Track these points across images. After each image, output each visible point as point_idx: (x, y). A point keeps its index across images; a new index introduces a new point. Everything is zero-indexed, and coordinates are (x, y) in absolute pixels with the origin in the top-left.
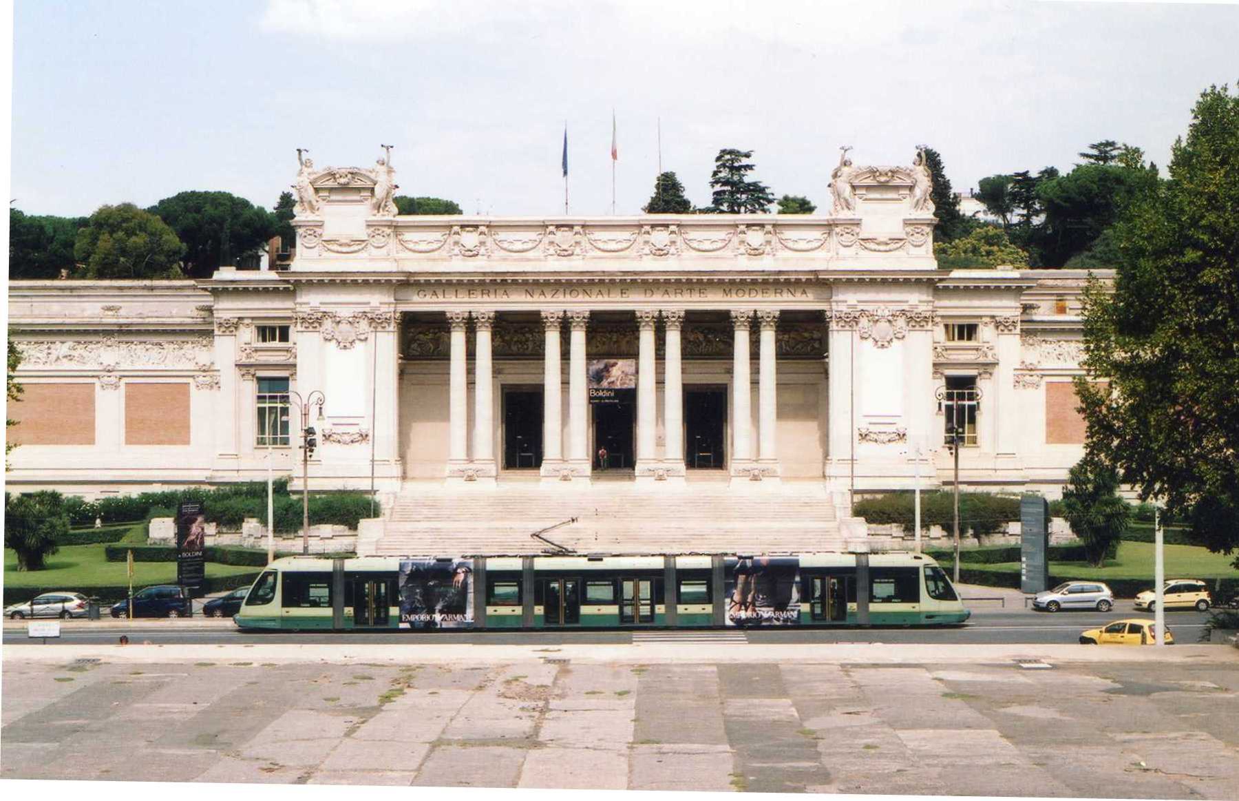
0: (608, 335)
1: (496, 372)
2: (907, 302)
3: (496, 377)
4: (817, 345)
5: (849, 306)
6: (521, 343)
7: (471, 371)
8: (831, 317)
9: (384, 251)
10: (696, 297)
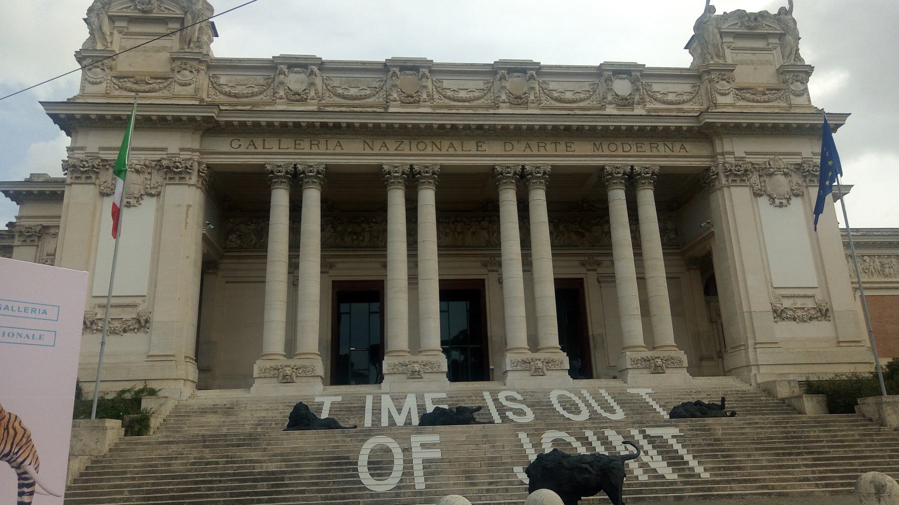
0: (452, 225)
1: (326, 266)
2: (799, 154)
3: (327, 273)
4: (672, 236)
5: (738, 159)
6: (355, 234)
7: (294, 266)
8: (717, 174)
9: (190, 90)
10: (561, 148)
